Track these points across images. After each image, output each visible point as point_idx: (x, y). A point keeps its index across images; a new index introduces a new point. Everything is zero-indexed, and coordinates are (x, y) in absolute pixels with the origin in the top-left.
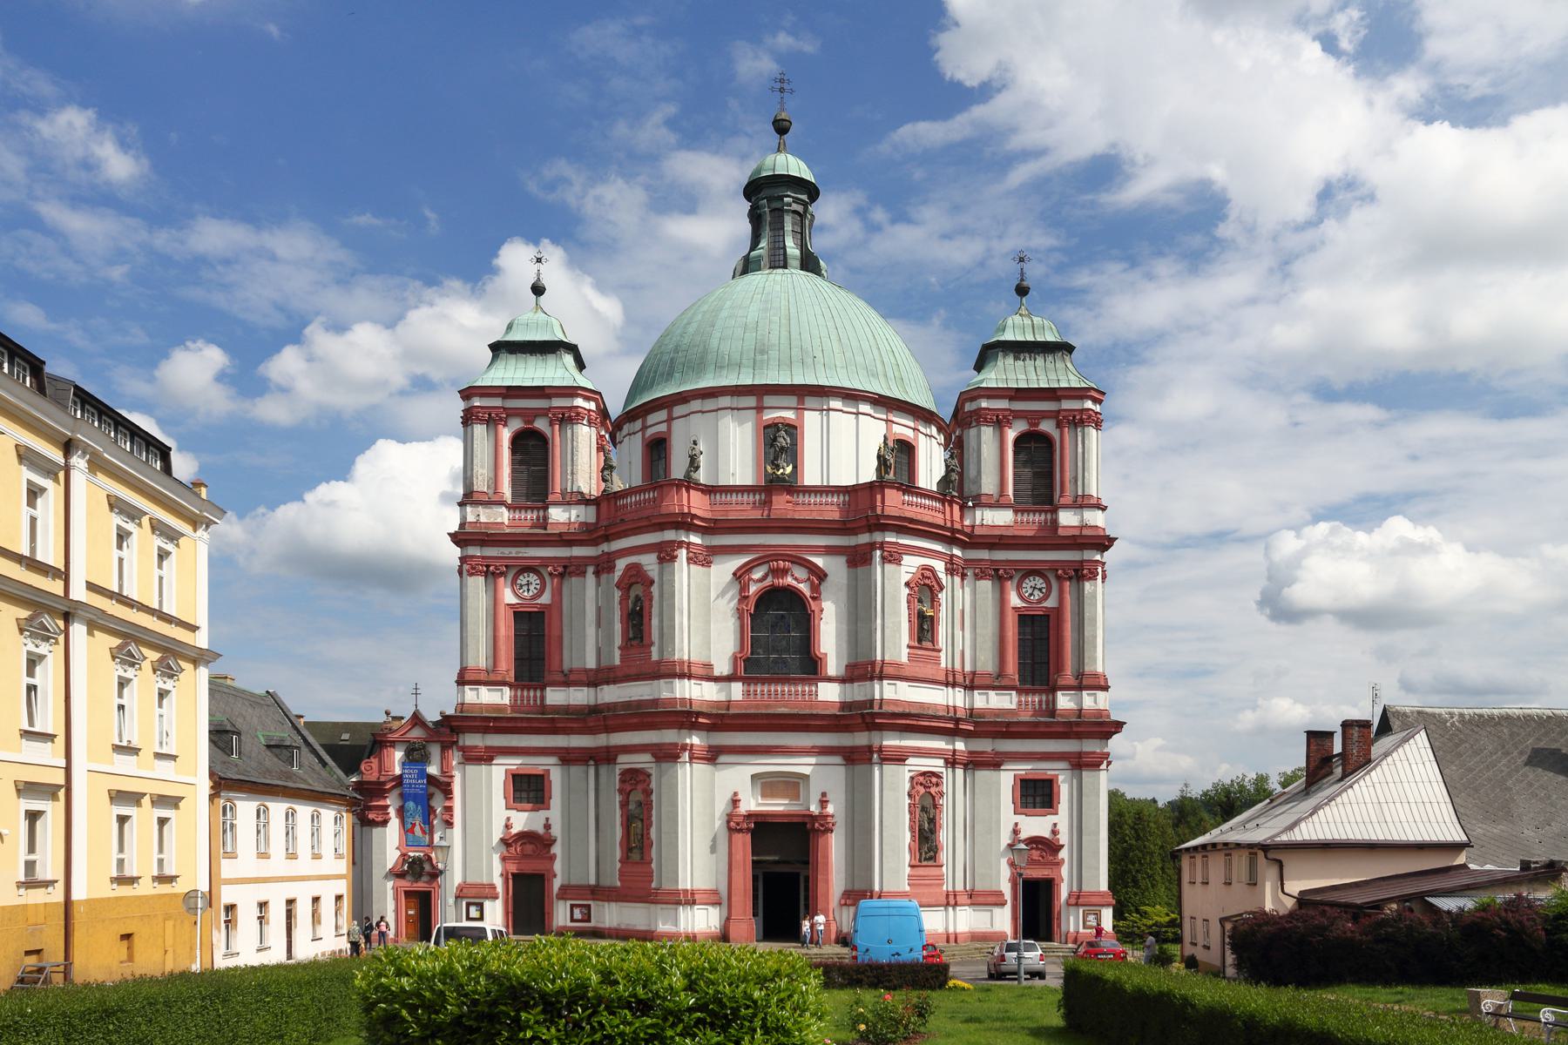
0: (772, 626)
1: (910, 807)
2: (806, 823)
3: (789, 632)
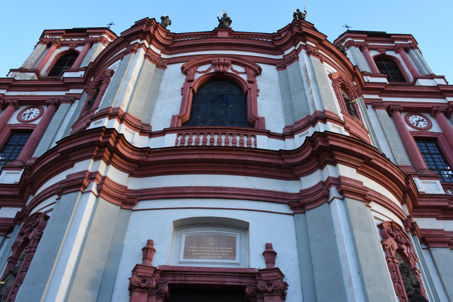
0: (212, 101)
1: (388, 262)
2: (245, 287)
3: (227, 105)
